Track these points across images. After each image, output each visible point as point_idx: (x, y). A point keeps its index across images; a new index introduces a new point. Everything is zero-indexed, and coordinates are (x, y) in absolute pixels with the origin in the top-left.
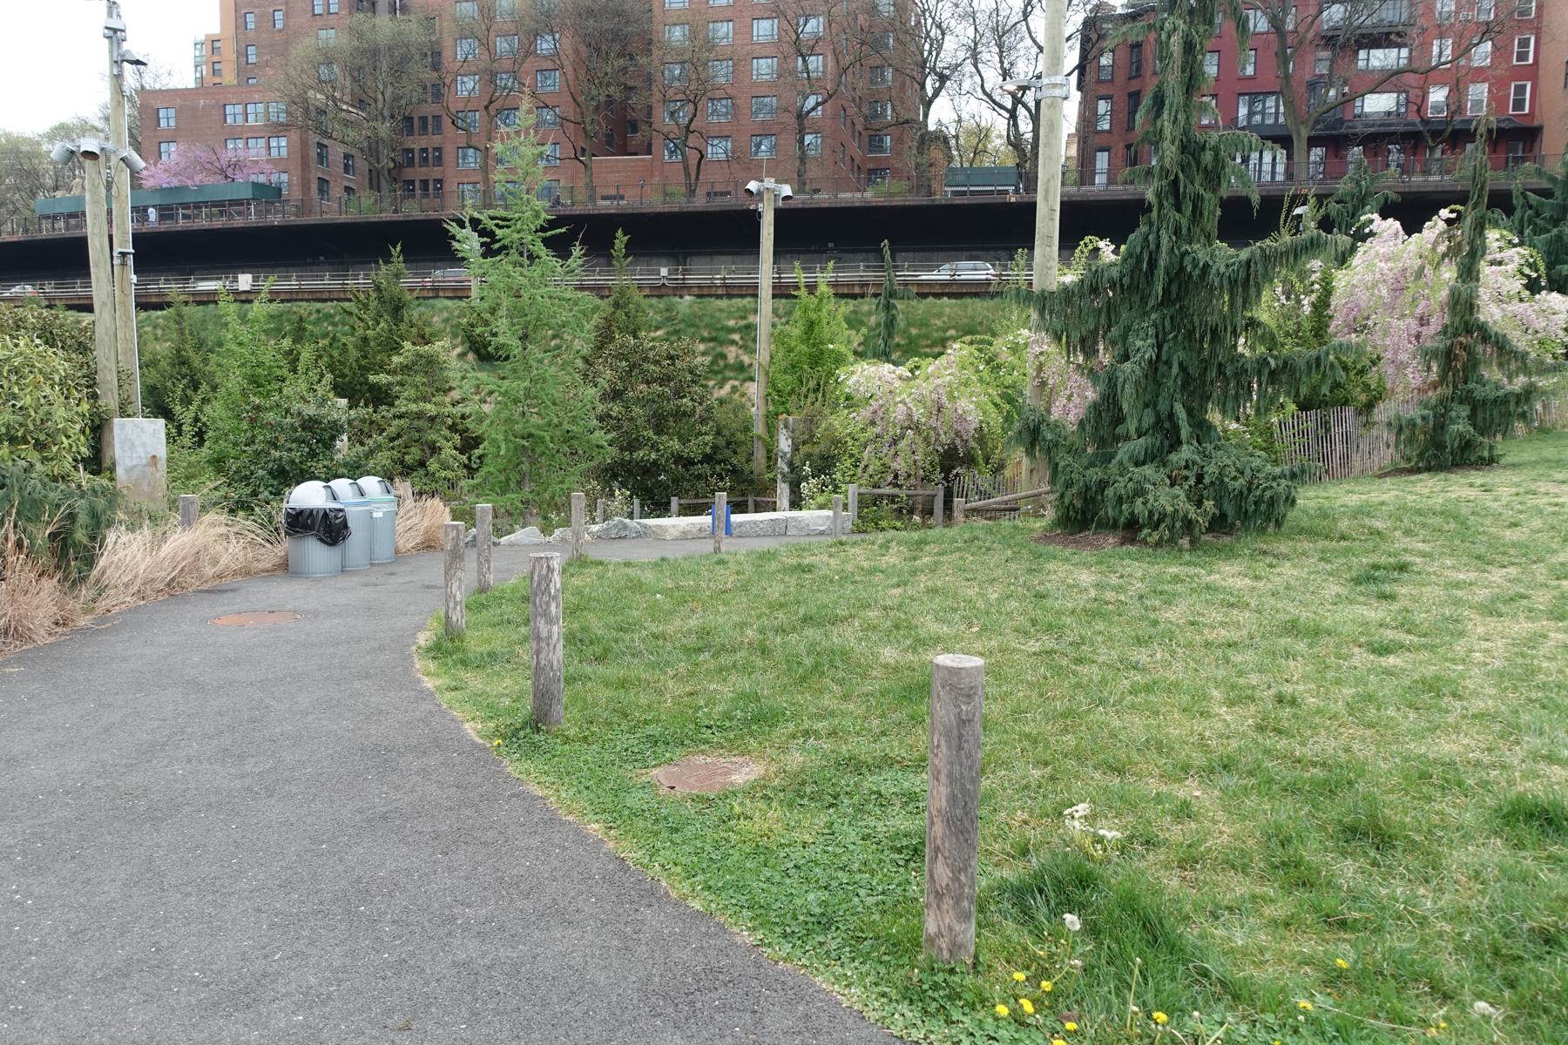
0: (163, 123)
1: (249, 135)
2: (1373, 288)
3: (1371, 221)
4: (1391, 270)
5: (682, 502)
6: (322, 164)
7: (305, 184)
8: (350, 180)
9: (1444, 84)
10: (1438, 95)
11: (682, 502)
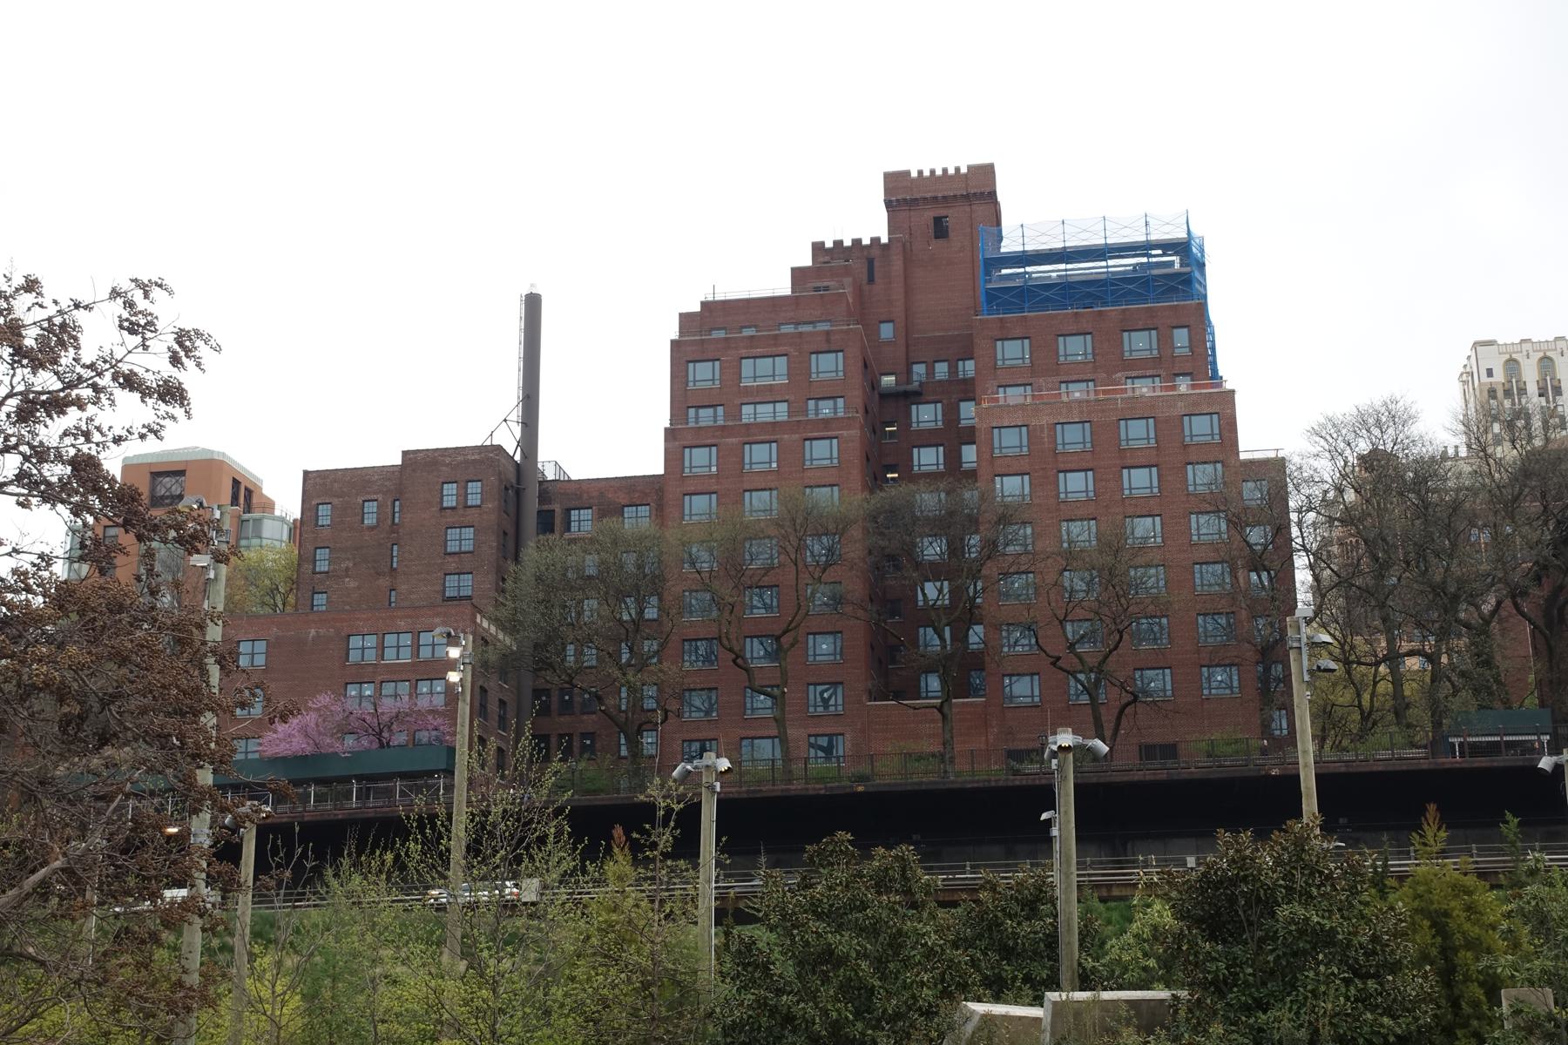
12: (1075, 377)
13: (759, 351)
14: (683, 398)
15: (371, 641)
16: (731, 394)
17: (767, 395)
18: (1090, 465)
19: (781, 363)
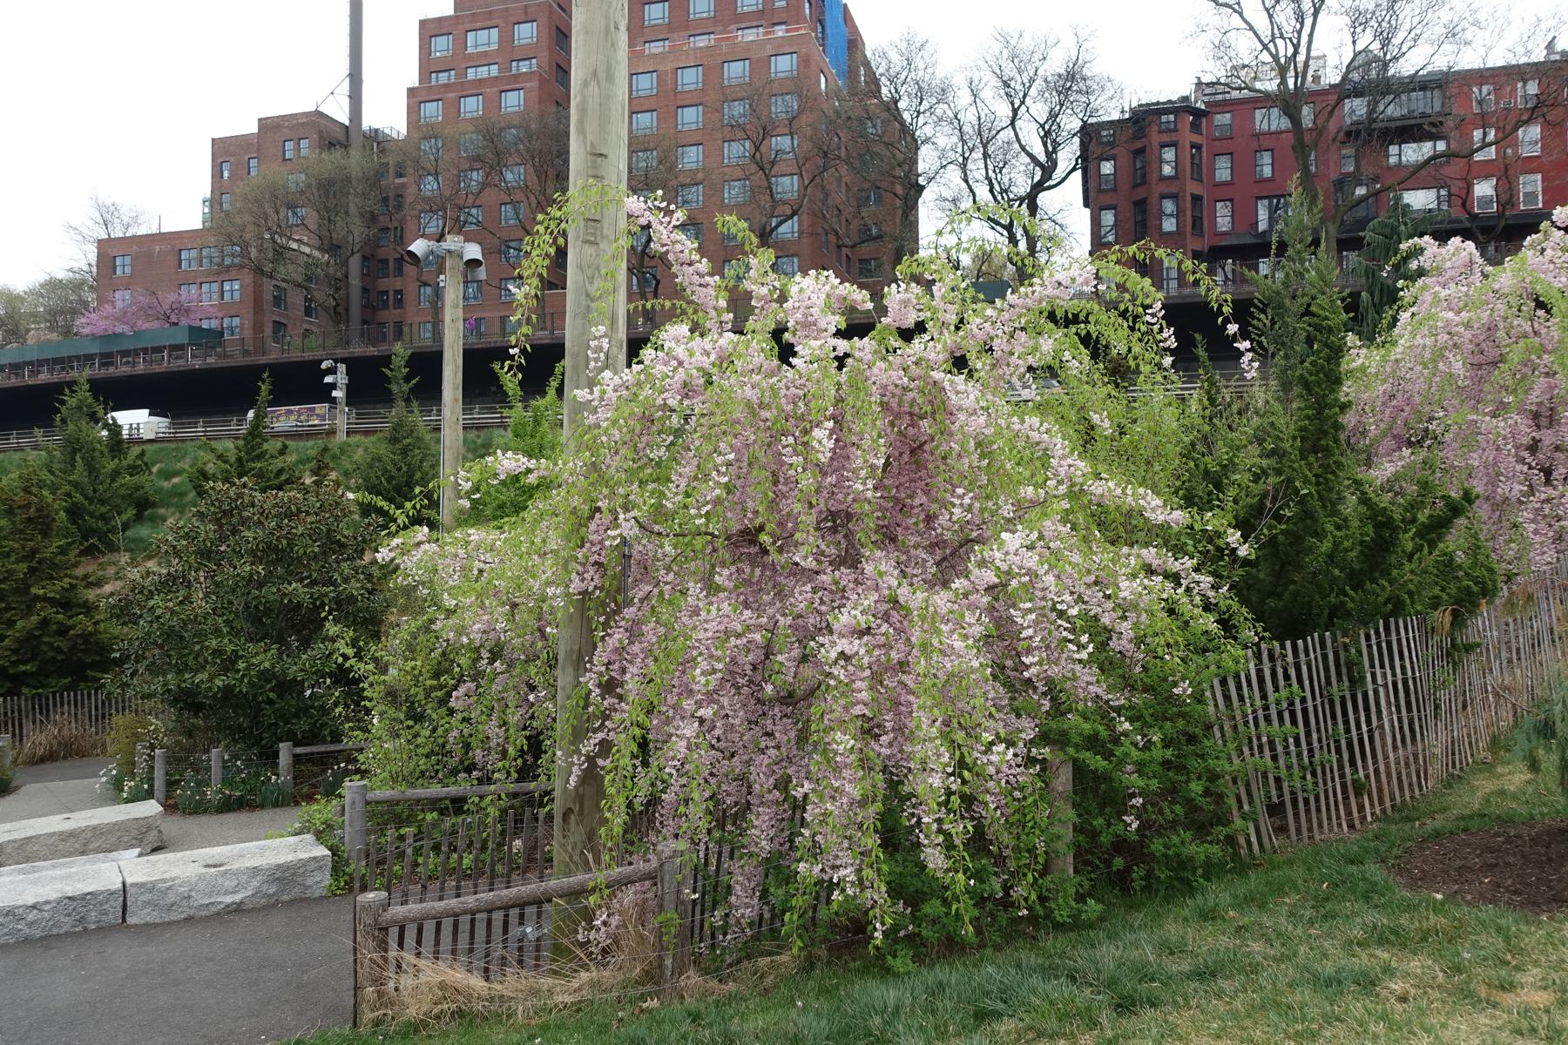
0: (119, 271)
1: (204, 280)
2: (1434, 361)
3: (1420, 251)
4: (1468, 325)
5: (299, 750)
6: (279, 307)
7: (258, 327)
8: (310, 323)
9: (1487, 177)
10: (1484, 189)
11: (299, 750)
12: (699, 31)
13: (478, 25)
14: (428, 66)
15: (194, 253)
16: (461, 60)
17: (484, 59)
18: (698, 101)
19: (495, 32)
